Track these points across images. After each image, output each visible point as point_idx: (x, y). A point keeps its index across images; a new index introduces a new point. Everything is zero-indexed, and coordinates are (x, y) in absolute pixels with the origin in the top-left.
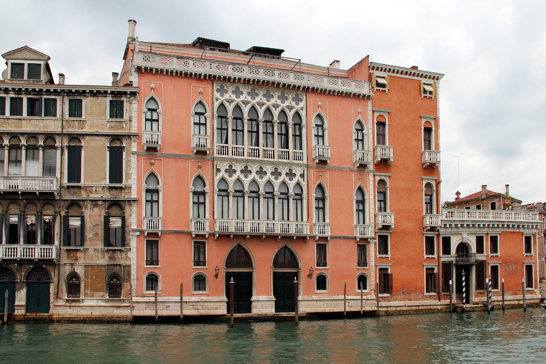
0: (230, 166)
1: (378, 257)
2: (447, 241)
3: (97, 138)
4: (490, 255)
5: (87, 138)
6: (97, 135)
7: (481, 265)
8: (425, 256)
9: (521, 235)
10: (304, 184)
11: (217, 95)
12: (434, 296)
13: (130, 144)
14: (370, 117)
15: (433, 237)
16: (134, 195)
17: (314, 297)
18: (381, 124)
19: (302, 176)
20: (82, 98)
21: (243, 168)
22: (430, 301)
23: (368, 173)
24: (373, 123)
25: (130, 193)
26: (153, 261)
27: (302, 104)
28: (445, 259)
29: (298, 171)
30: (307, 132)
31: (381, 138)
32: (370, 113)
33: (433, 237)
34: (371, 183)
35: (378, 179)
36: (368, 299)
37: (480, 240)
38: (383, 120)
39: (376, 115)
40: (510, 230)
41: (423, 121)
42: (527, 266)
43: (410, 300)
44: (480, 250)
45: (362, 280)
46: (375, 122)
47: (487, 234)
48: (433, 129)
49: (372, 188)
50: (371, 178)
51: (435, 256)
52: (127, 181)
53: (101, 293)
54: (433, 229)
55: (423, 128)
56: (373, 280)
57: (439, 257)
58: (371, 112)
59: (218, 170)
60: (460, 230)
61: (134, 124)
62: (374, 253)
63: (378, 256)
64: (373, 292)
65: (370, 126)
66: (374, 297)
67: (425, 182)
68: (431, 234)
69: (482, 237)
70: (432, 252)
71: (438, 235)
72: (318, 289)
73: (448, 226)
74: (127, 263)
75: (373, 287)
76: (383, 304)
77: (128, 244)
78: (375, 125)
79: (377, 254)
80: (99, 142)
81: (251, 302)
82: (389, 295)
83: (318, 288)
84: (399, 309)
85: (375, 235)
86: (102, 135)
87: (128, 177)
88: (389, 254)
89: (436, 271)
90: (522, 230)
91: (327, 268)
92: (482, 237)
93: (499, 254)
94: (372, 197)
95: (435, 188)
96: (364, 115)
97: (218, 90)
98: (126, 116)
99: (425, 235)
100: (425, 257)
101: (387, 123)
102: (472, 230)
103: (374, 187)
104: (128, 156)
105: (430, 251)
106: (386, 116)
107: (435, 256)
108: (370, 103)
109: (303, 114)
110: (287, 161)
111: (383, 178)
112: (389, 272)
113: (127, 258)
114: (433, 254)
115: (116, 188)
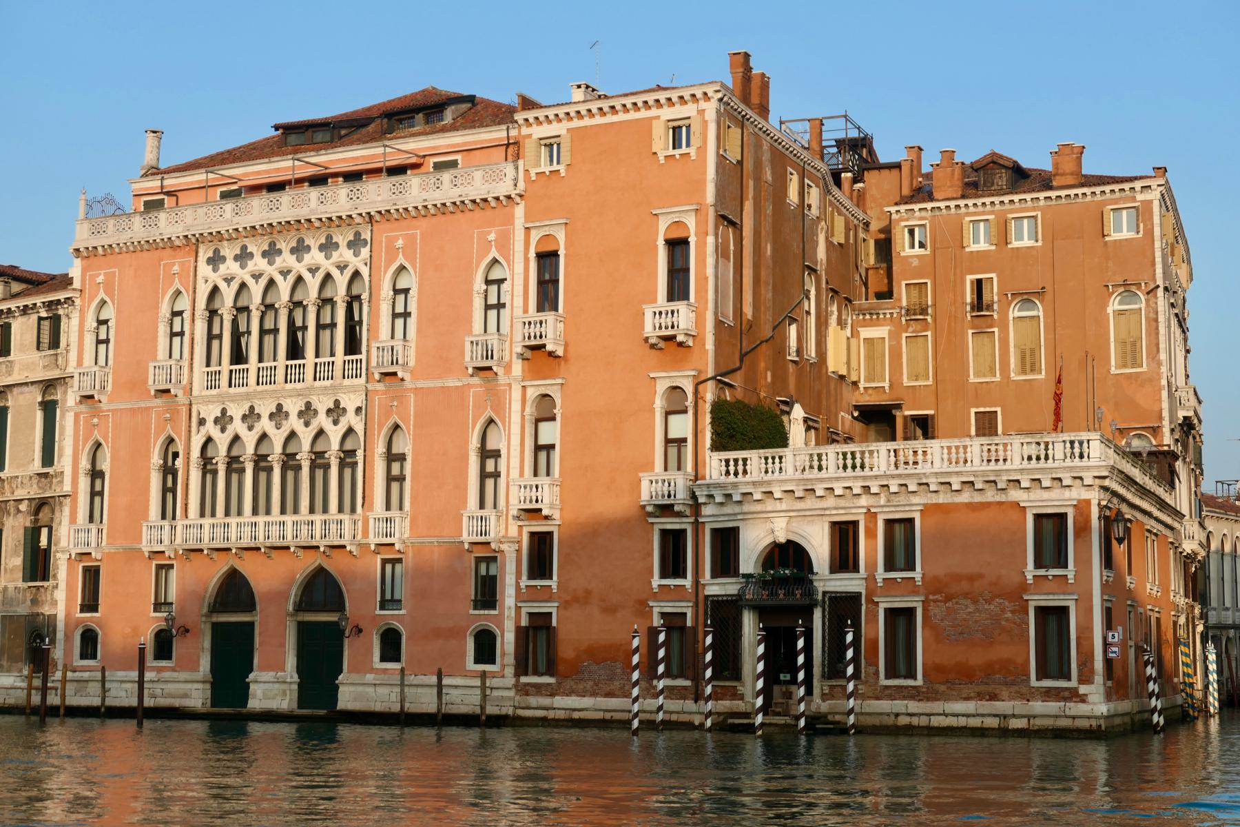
0: (224, 411)
1: (523, 585)
2: (726, 541)
3: (25, 389)
4: (881, 574)
5: (15, 390)
6: (26, 384)
7: (845, 609)
8: (656, 581)
9: (1015, 515)
10: (359, 429)
11: (204, 270)
12: (685, 688)
13: (65, 392)
14: (519, 246)
15: (685, 531)
16: (67, 488)
17: (370, 677)
18: (547, 258)
19: (358, 410)
20: (11, 320)
21: (245, 408)
22: (660, 701)
23: (510, 385)
24: (527, 260)
25: (61, 482)
26: (90, 604)
27: (365, 252)
28: (719, 588)
29: (350, 402)
30: (369, 313)
31: (547, 295)
32: (519, 235)
33: (685, 531)
34: (516, 406)
35: (532, 393)
36: (502, 687)
37: (844, 534)
38: (549, 248)
39: (535, 236)
40: (965, 497)
41: (663, 225)
42: (1042, 612)
43: (609, 695)
44: (844, 559)
45: (486, 647)
46: (532, 255)
47: (871, 516)
48: (692, 240)
49: (516, 418)
50: (516, 394)
51: (687, 582)
52: (59, 462)
53: (20, 665)
54: (666, 510)
55: (661, 243)
56: (507, 641)
57: (696, 583)
58: (523, 231)
59: (202, 422)
60: (770, 505)
61: (73, 356)
62: (513, 577)
63: (525, 582)
64: (509, 671)
65: (519, 268)
66: (510, 681)
67: (662, 387)
68: (672, 524)
69: (855, 524)
70: (679, 572)
71: (697, 526)
72: (383, 659)
73: (719, 499)
74: (52, 612)
75: (510, 659)
76: (533, 701)
77: (55, 576)
78: (533, 266)
79: (524, 577)
80: (28, 396)
81: (247, 686)
82: (552, 680)
83: (383, 659)
84: (576, 715)
85: (520, 533)
86: (32, 383)
87: (60, 456)
88: (555, 577)
89: (689, 623)
90: (1015, 495)
91: (401, 612)
92: (855, 524)
93: (917, 575)
94: (515, 440)
95: (690, 402)
96: (504, 243)
97: (210, 261)
98: (63, 343)
99: (657, 528)
100: (656, 581)
101: (562, 253)
102: (810, 503)
103: (523, 417)
104: (63, 416)
105: (673, 564)
106: (561, 236)
107: (687, 582)
108: (519, 211)
109: (365, 272)
110: (328, 383)
111: (543, 391)
112: (554, 623)
113: (54, 603)
114: (679, 572)
115: (46, 475)
